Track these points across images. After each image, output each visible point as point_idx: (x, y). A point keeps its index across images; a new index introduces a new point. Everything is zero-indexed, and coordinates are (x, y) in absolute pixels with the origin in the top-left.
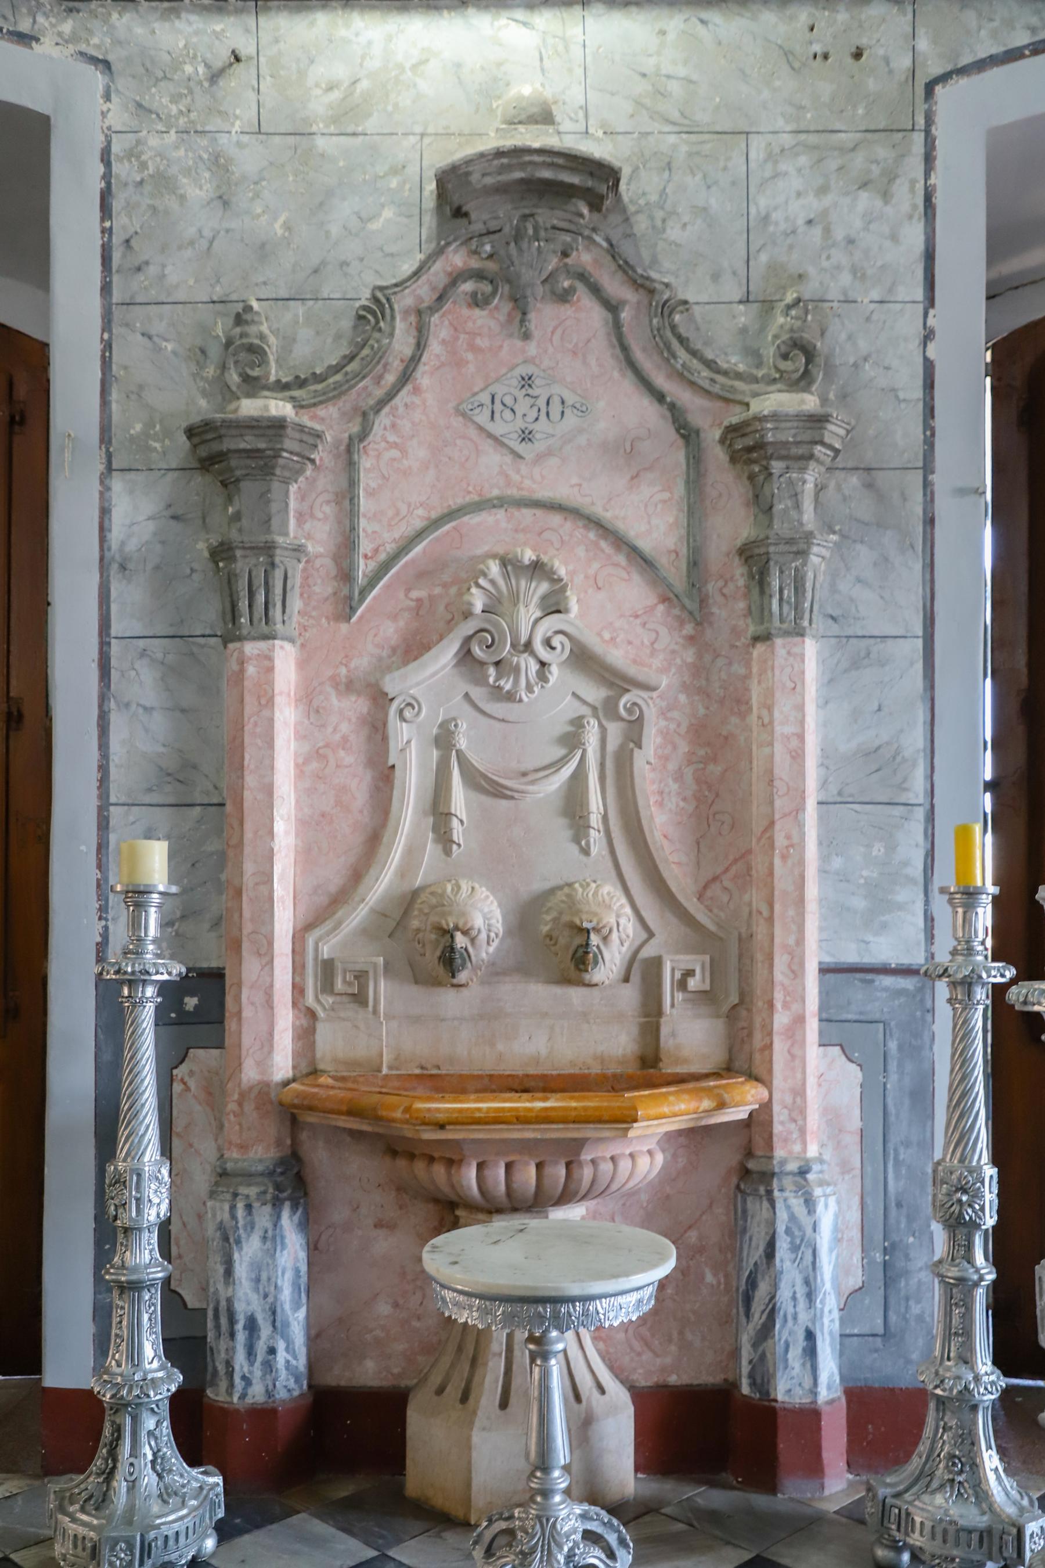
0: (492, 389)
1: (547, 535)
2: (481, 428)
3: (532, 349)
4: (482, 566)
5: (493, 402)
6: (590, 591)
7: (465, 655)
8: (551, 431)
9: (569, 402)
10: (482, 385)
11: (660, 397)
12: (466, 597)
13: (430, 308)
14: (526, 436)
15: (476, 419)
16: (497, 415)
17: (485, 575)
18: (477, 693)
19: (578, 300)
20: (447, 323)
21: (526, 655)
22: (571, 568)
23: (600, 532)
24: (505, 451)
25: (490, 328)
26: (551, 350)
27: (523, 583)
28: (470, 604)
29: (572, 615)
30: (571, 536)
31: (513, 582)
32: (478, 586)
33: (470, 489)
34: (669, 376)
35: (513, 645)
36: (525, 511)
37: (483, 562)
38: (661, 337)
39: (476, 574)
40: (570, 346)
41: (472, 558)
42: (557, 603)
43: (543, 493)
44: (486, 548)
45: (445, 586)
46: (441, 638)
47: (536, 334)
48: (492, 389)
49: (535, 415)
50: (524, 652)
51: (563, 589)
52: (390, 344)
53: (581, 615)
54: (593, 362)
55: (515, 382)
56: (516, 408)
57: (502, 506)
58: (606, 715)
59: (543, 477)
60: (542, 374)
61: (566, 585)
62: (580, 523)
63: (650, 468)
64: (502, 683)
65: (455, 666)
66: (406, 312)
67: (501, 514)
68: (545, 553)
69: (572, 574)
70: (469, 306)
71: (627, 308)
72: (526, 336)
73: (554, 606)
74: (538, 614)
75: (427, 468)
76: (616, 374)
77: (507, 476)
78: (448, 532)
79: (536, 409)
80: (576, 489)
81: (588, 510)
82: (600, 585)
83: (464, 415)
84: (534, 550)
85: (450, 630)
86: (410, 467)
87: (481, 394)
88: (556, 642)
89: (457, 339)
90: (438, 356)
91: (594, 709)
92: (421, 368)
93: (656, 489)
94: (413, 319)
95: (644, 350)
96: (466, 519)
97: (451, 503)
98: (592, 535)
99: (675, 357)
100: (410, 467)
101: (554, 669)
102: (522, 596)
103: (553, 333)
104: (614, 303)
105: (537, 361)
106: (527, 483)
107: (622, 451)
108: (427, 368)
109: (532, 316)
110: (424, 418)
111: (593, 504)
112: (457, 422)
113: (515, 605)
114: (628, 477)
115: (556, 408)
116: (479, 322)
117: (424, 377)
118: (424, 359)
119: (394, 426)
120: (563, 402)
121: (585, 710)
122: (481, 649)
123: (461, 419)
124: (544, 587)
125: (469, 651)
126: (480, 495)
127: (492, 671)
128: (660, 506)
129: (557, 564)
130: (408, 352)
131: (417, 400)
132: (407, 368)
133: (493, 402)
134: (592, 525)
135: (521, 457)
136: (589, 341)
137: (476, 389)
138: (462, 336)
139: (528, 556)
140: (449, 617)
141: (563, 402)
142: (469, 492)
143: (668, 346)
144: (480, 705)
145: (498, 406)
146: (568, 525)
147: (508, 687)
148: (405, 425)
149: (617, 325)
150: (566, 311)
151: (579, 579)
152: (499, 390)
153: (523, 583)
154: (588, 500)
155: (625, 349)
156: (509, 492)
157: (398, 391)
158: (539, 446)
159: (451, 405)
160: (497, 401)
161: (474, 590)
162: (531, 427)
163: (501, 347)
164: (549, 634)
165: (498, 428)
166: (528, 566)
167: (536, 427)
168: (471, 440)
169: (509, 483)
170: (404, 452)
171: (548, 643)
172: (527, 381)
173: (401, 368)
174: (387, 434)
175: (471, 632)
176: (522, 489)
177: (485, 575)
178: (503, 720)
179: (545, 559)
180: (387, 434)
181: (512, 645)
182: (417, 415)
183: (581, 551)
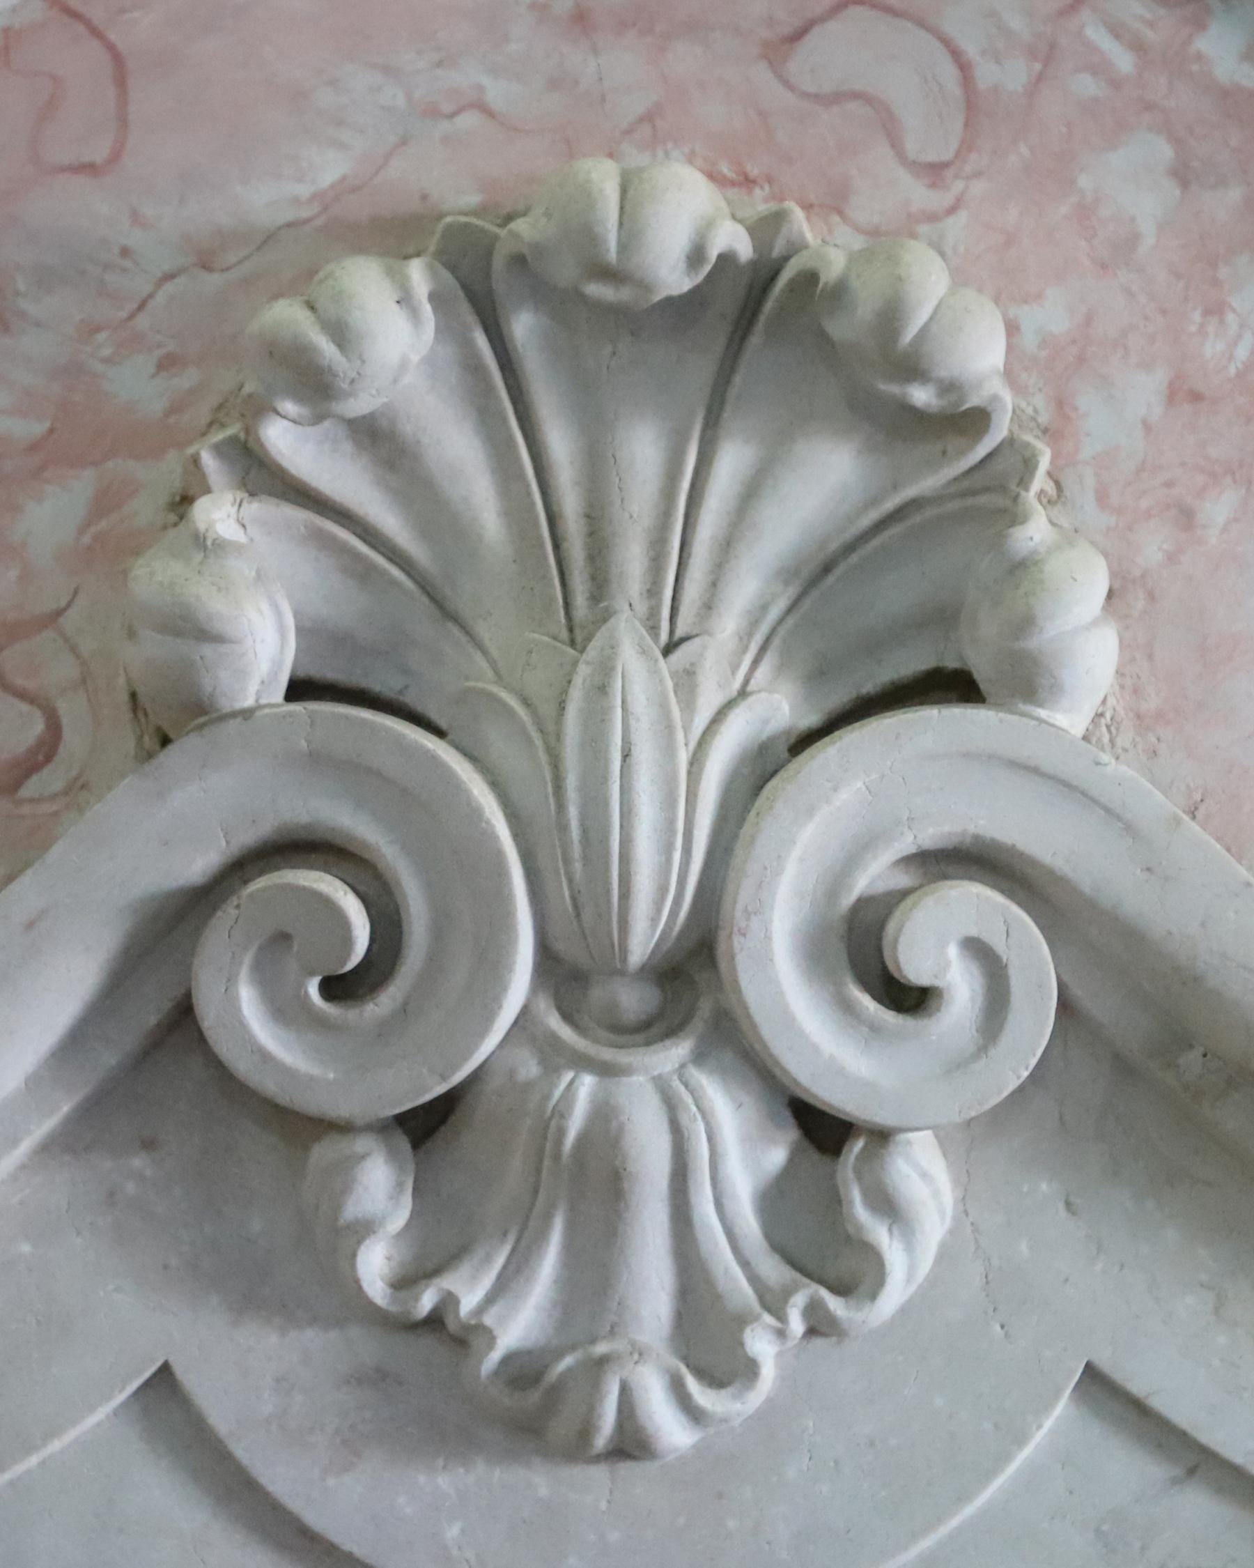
4: (287, 315)
7: (149, 1059)
12: (157, 575)
17: (315, 386)
18: (250, 1375)
21: (672, 1055)
22: (1051, 316)
27: (642, 450)
28: (192, 629)
29: (1070, 718)
30: (1046, 55)
31: (560, 444)
32: (262, 476)
35: (560, 974)
37: (304, 283)
39: (241, 380)
42: (943, 617)
44: (329, 168)
50: (655, 1028)
51: (991, 496)
53: (1151, 713)
61: (1011, 466)
64: (469, 1290)
65: (68, 1143)
68: (833, 203)
69: (1062, 367)
73: (910, 646)
74: (779, 707)
84: (736, 183)
88: (936, 938)
101: (923, 1173)
102: (632, 560)
113: (576, 637)
122: (285, 1010)
124: (825, 481)
127: (379, 1187)
129: (929, 284)
139: (685, 222)
144: (282, 1478)
147: (519, 1326)
151: (1121, 412)
153: (642, 450)
161: (222, 513)
164: (874, 875)
166: (694, 301)
175: (199, 865)
177: (315, 386)
179: (828, 248)
181: (546, 954)
183: (1131, 183)
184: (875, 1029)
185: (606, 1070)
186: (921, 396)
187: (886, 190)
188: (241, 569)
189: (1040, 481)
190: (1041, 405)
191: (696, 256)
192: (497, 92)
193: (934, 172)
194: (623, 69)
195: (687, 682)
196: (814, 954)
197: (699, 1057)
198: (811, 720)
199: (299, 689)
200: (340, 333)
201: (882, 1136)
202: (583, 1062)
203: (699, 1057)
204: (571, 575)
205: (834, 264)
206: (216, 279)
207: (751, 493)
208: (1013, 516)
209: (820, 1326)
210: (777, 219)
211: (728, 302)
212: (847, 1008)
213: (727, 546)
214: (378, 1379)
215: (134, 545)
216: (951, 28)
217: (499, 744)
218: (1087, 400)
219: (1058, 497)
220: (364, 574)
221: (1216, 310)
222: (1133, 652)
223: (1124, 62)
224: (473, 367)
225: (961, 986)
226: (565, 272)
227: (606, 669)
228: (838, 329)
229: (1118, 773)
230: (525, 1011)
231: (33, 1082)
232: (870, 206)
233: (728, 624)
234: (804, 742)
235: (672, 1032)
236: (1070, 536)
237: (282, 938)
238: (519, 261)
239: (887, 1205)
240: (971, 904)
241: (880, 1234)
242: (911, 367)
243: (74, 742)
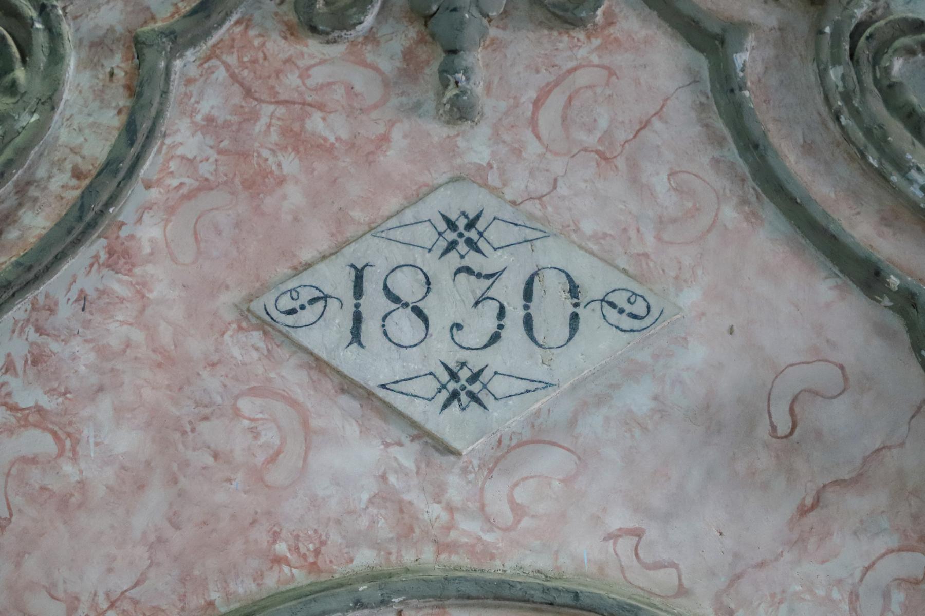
0: (356, 253)
2: (319, 365)
3: (477, 145)
5: (358, 290)
8: (539, 373)
9: (593, 288)
10: (325, 245)
11: (867, 275)
13: (171, 34)
14: (463, 387)
15: (301, 336)
16: (371, 328)
19: (610, 21)
20: (221, 74)
24: (395, 431)
25: (350, 88)
26: (533, 148)
33: (281, 548)
34: (887, 220)
38: (856, 114)
40: (591, 140)
47: (490, 106)
48: (356, 253)
49: (491, 325)
52: (42, 127)
54: (660, 183)
55: (426, 235)
56: (427, 307)
59: (518, 510)
60: (508, 213)
63: (858, 481)
66: (99, 45)
70: (290, 32)
71: (750, 41)
72: (460, 111)
75: (141, 486)
76: (730, 214)
77: (402, 507)
79: (491, 309)
80: (625, 545)
83: (266, 325)
86: (82, 484)
87: (322, 267)
89: (253, 116)
90: (190, 162)
92: (136, 195)
93: (881, 544)
94: (118, 62)
95: (808, 149)
99: (902, 167)
100: (82, 484)
103: (537, 104)
104: (717, 30)
105: (493, 179)
107: (763, 431)
108: (154, 194)
109: (476, 58)
110: (138, 336)
111: (682, 591)
112: (246, 348)
114: (789, 509)
115: (552, 307)
116: (319, 75)
117: (144, 221)
118: (146, 170)
119: (37, 359)
120: (574, 290)
123: (256, 337)
126: (313, 568)
128: (898, 596)
130: (98, 150)
131: (118, 285)
132: (90, 192)
133: (358, 290)
135: (448, 450)
136: (645, 125)
137: (306, 255)
138: (267, 109)
141: (574, 290)
142: (278, 560)
143: (881, 143)
145: (374, 302)
148: (78, 358)
149: (726, 87)
150: (576, 49)
152: (379, 255)
154: (667, 577)
155: (752, 146)
156: (408, 558)
157: (60, 258)
158: (505, 416)
159: (227, 299)
160: (372, 286)
162: (476, 361)
163: (385, 138)
165: (374, 365)
167: (494, 359)
168: (292, 402)
169: (407, 527)
170: (67, 440)
172: (462, 233)
173: (72, 195)
174: (14, 383)
176: (451, 547)
180: (14, 383)
182: (117, 329)
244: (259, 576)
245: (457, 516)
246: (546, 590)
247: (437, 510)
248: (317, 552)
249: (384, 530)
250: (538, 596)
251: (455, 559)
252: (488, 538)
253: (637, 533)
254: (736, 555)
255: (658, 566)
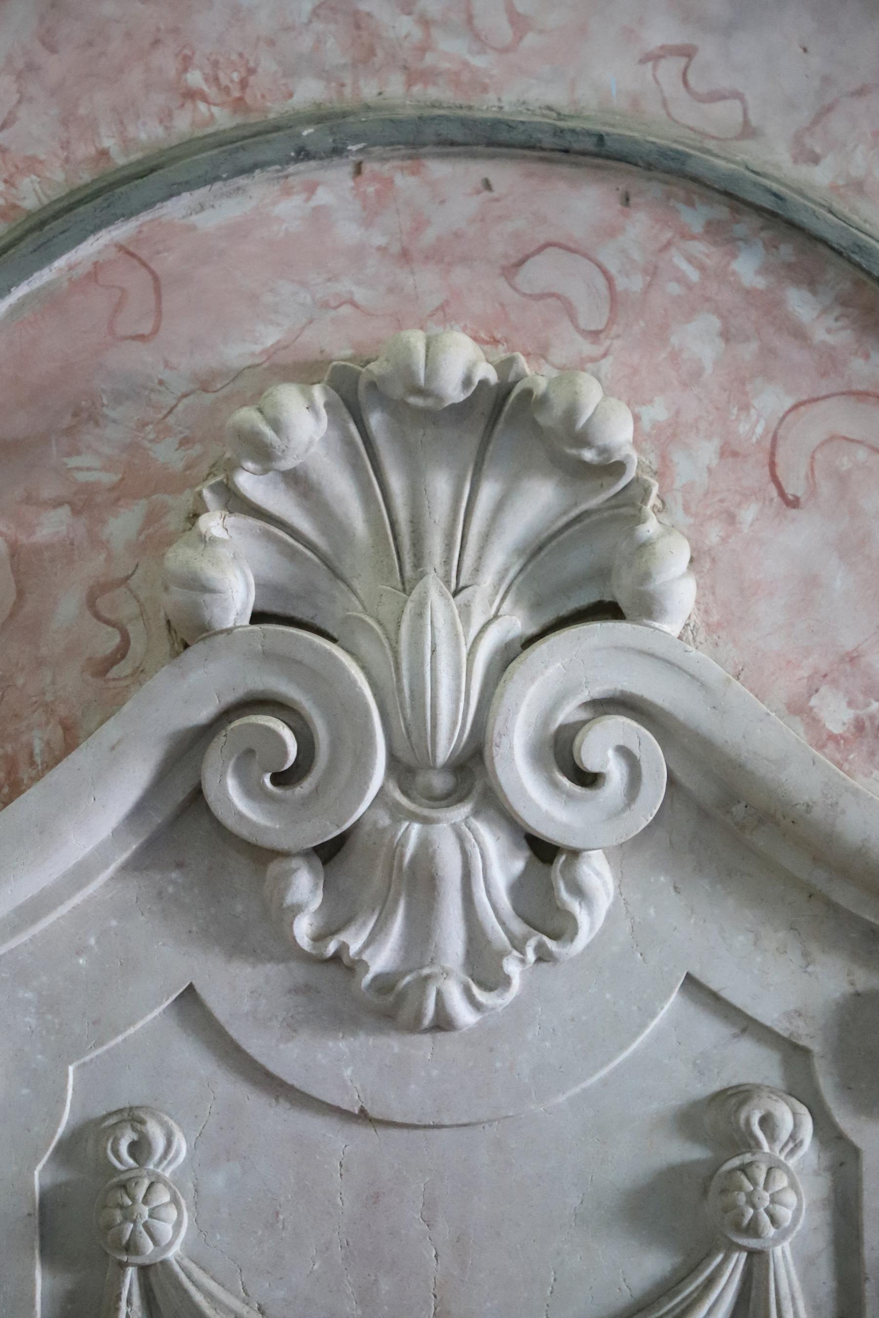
1: (540, 273)
4: (248, 416)
6: (748, 514)
7: (180, 823)
12: (179, 557)
17: (264, 454)
18: (237, 989)
21: (461, 812)
22: (657, 412)
23: (786, 251)
27: (440, 486)
28: (199, 586)
29: (671, 627)
30: (653, 272)
31: (396, 483)
32: (236, 502)
33: (195, 78)
35: (401, 770)
36: (439, 169)
37: (256, 397)
39: (223, 452)
41: (204, 384)
42: (603, 573)
43: (524, 92)
44: (271, 336)
45: (85, 503)
46: (70, 738)
50: (452, 798)
51: (627, 508)
53: (713, 624)
57: (337, 151)
58: (847, 1085)
62: (694, 218)
64: (354, 941)
65: (135, 866)
67: (333, 187)
68: (541, 353)
69: (664, 439)
74: (515, 623)
78: (95, 272)
81: (734, 158)
82: (794, 486)
84: (487, 341)
85: (110, 705)
91: (793, 1052)
96: (175, 209)
97: (108, 143)
98: (747, 268)
101: (598, 873)
102: (435, 544)
106: (451, 48)
111: (748, 131)
113: (406, 587)
121: (752, 1064)
122: (252, 791)
124: (539, 501)
125: (197, 796)
126: (239, 105)
127: (305, 887)
129: (591, 395)
134: (746, 225)
139: (461, 363)
140: (109, 641)
142: (191, 95)
144: (255, 1046)
146: (640, 228)
147: (381, 960)
151: (696, 462)
153: (440, 486)
154: (726, 114)
156: (369, 91)
161: (214, 523)
164: (568, 713)
169: (366, 49)
171: (563, 758)
175: (204, 714)
176: (427, 76)
177: (264, 454)
178: (363, 1117)
179: (538, 377)
181: (393, 760)
183: (698, 340)
184: (570, 796)
185: (426, 821)
186: (589, 455)
187: (569, 346)
188: (224, 553)
189: (653, 500)
190: (653, 460)
191: (467, 382)
192: (360, 295)
193: (594, 335)
194: (427, 282)
195: (466, 611)
196: (537, 757)
197: (476, 813)
198: (533, 630)
199: (257, 617)
200: (276, 425)
201: (575, 854)
202: (413, 817)
203: (476, 813)
204: (404, 555)
205: (541, 385)
206: (209, 398)
207: (499, 507)
208: (639, 519)
209: (543, 956)
210: (510, 362)
211: (485, 406)
212: (555, 785)
213: (486, 538)
214: (305, 990)
215: (168, 541)
216: (602, 258)
217: (365, 645)
218: (678, 457)
219: (663, 508)
220: (291, 554)
221: (745, 407)
222: (705, 590)
223: (694, 275)
224: (348, 442)
225: (616, 773)
226: (397, 391)
227: (422, 604)
228: (543, 419)
229: (697, 656)
230: (382, 789)
231: (115, 832)
232: (558, 355)
233: (488, 579)
234: (529, 642)
235: (461, 800)
236: (669, 530)
237: (250, 752)
238: (372, 385)
239: (578, 891)
240: (619, 728)
241: (575, 906)
242: (583, 440)
243: (137, 647)
244: (166, 117)
245: (436, 33)
246: (559, 132)
247: (405, 27)
248: (244, 84)
249: (334, 53)
250: (548, 141)
251: (434, 93)
252: (478, 62)
253: (687, 52)
254: (826, 80)
255: (715, 97)
